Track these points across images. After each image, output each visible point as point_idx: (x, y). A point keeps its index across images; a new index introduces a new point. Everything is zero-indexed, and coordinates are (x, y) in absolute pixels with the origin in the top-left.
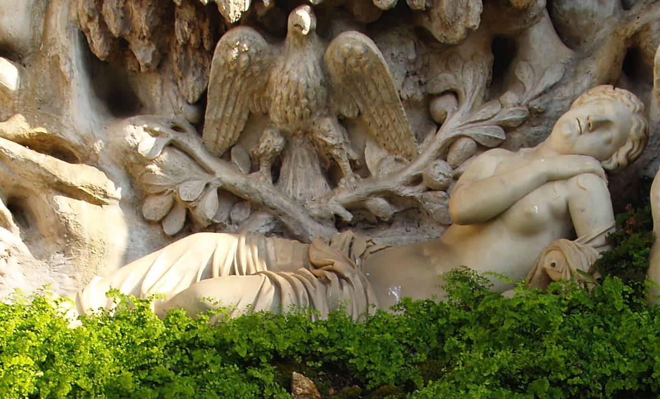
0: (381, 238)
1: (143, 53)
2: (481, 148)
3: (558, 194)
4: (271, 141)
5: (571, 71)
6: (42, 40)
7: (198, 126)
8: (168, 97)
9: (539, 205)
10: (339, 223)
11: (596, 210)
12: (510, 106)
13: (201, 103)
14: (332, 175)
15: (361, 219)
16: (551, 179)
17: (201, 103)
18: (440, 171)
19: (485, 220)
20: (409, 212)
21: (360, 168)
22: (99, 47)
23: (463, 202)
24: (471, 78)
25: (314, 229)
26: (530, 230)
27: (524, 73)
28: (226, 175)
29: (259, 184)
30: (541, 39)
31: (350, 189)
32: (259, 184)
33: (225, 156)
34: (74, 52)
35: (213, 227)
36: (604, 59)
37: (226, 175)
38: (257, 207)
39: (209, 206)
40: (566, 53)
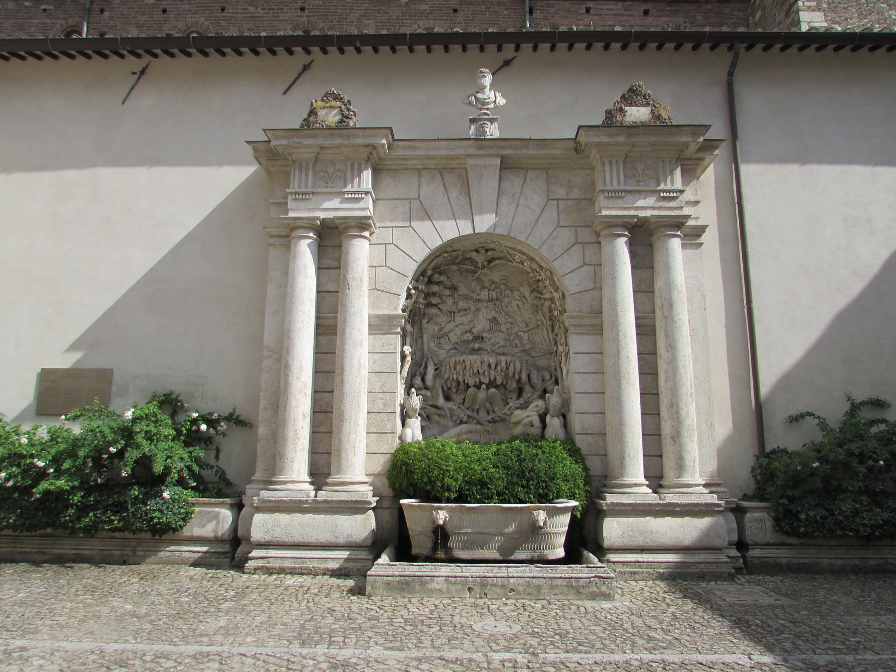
0: (498, 425)
1: (454, 390)
2: (517, 408)
3: (530, 419)
4: (477, 407)
5: (533, 394)
6: (434, 387)
7: (463, 403)
8: (458, 398)
9: (526, 421)
10: (489, 422)
11: (536, 420)
12: (522, 401)
13: (464, 400)
14: (488, 413)
15: (493, 421)
16: (528, 416)
17: (464, 400)
18: (509, 413)
19: (517, 423)
20: (503, 420)
21: (493, 412)
22: (445, 389)
23: (513, 420)
24: (514, 396)
25: (485, 423)
26: (525, 425)
27: (524, 394)
28: (468, 413)
29: (474, 415)
30: (527, 388)
31: (491, 416)
32: (474, 415)
33: (468, 409)
34: (441, 389)
35: (466, 423)
36: (537, 394)
37: (468, 413)
38: (474, 418)
39: (465, 419)
40: (532, 390)
